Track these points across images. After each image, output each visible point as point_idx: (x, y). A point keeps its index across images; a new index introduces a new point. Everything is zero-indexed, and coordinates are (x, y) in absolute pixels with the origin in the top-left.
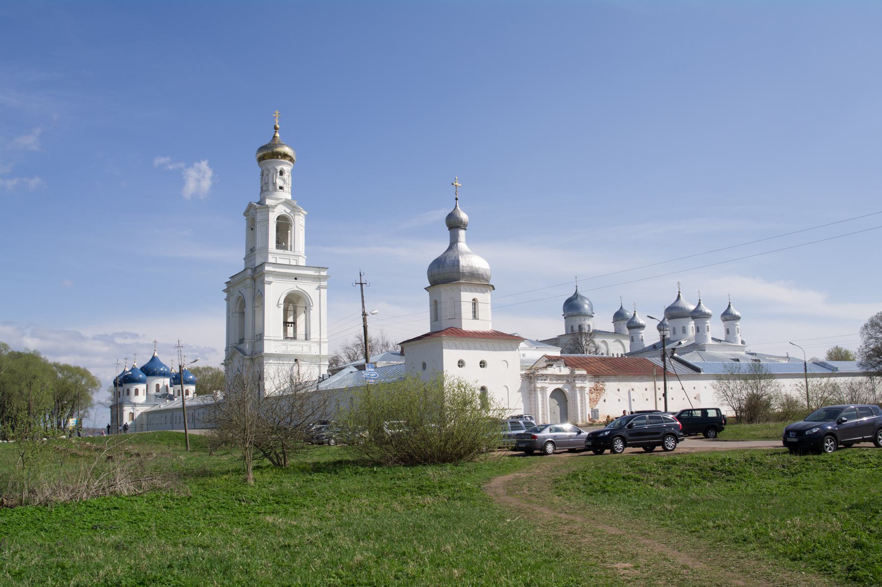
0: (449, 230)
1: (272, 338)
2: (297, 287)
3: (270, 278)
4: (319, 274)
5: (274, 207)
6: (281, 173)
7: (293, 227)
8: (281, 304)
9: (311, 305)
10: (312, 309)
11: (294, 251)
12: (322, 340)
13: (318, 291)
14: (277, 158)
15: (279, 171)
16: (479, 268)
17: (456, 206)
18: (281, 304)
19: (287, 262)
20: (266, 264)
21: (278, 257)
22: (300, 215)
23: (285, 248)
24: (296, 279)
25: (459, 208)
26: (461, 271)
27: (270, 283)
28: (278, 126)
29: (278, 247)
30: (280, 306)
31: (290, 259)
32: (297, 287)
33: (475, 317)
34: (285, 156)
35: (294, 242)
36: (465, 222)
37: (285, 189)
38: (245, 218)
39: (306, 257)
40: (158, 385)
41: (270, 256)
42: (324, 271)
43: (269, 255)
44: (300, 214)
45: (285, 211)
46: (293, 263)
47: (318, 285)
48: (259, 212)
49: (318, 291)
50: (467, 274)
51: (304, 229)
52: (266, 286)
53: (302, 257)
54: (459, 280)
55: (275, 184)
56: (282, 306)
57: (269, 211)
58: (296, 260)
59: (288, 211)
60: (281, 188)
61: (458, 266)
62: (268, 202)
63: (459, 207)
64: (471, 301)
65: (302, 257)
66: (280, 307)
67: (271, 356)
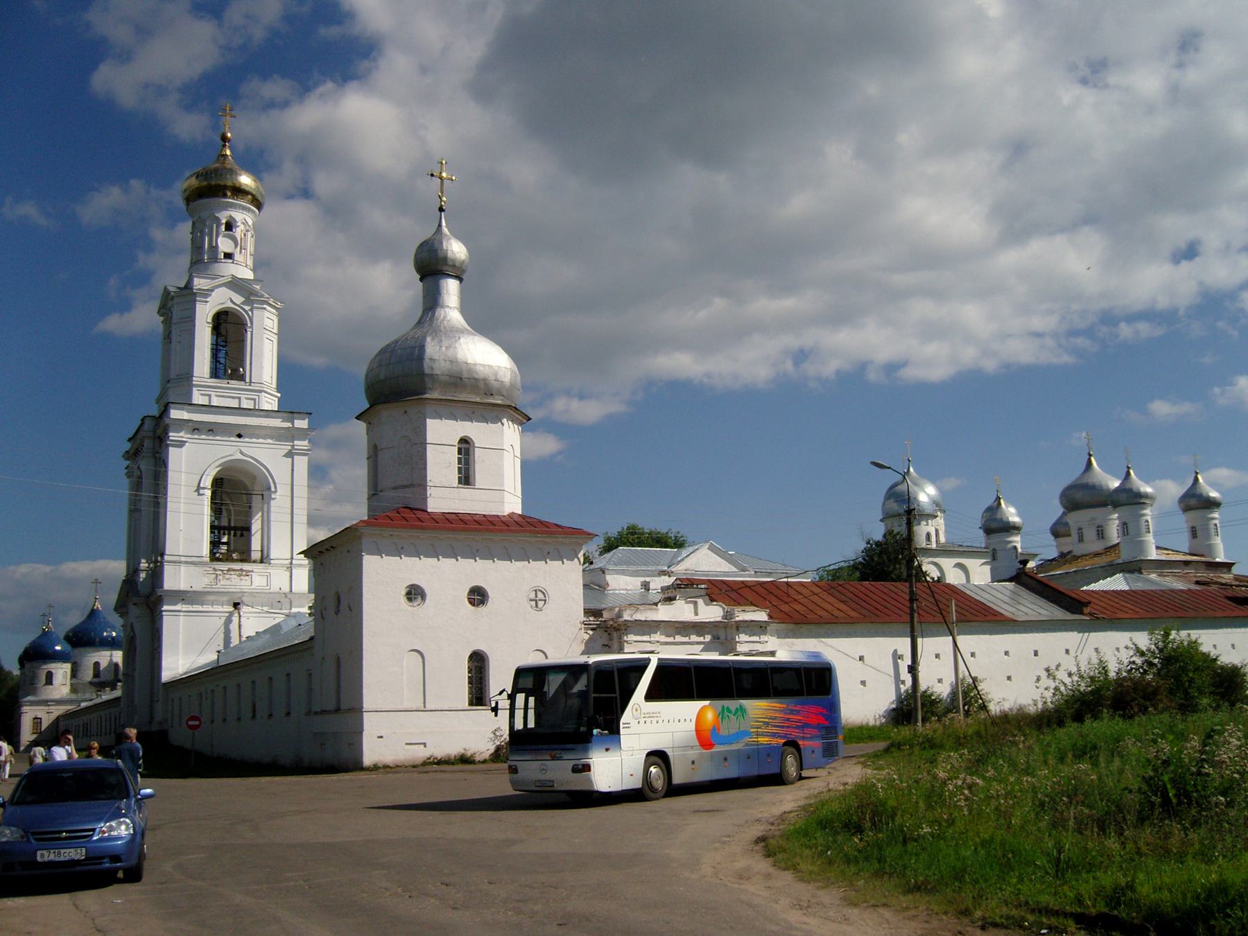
0: (421, 280)
1: (183, 559)
2: (242, 453)
3: (182, 434)
4: (289, 425)
5: (206, 293)
6: (230, 226)
7: (249, 333)
8: (204, 488)
9: (273, 489)
10: (274, 499)
11: (251, 382)
12: (294, 562)
13: (290, 459)
14: (225, 196)
15: (224, 221)
16: (476, 365)
17: (440, 225)
18: (204, 488)
19: (234, 404)
20: (171, 405)
21: (213, 394)
22: (265, 309)
23: (241, 378)
24: (239, 436)
25: (445, 230)
26: (427, 371)
27: (181, 444)
28: (229, 135)
29: (215, 374)
30: (201, 491)
31: (239, 398)
32: (242, 453)
33: (466, 478)
34: (239, 191)
35: (251, 363)
36: (453, 261)
37: (237, 257)
38: (162, 318)
39: (279, 395)
40: (97, 664)
41: (196, 393)
42: (304, 419)
43: (194, 389)
44: (265, 306)
45: (232, 301)
46: (246, 404)
47: (290, 448)
48: (177, 304)
49: (290, 459)
50: (443, 378)
51: (275, 339)
52: (172, 451)
53: (266, 392)
54: (425, 393)
55: (214, 249)
56: (208, 493)
57: (195, 301)
58: (254, 400)
59: (239, 299)
60: (228, 256)
61: (421, 358)
62: (199, 283)
63: (447, 227)
64: (456, 444)
65: (266, 392)
66: (203, 494)
67: (181, 596)
